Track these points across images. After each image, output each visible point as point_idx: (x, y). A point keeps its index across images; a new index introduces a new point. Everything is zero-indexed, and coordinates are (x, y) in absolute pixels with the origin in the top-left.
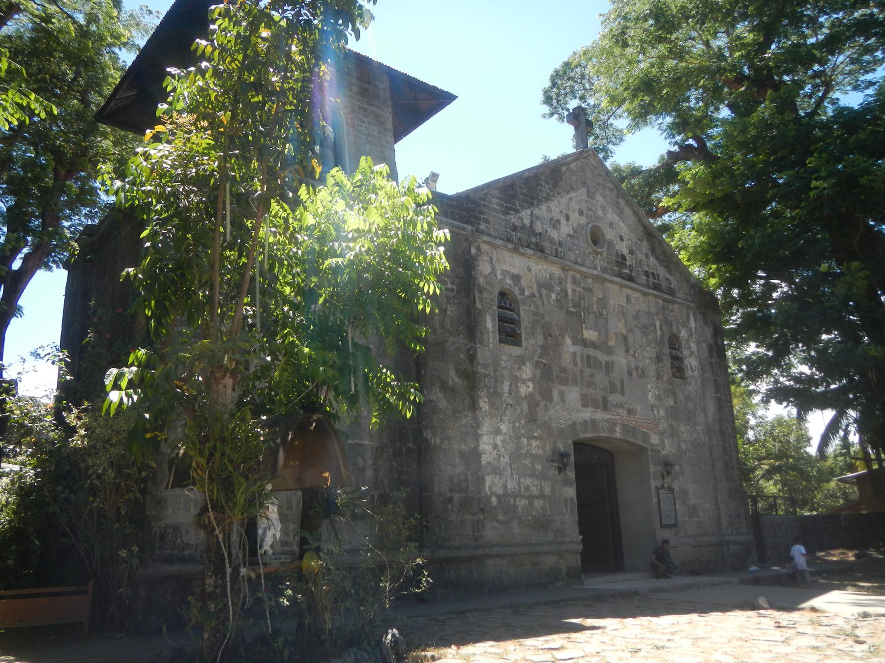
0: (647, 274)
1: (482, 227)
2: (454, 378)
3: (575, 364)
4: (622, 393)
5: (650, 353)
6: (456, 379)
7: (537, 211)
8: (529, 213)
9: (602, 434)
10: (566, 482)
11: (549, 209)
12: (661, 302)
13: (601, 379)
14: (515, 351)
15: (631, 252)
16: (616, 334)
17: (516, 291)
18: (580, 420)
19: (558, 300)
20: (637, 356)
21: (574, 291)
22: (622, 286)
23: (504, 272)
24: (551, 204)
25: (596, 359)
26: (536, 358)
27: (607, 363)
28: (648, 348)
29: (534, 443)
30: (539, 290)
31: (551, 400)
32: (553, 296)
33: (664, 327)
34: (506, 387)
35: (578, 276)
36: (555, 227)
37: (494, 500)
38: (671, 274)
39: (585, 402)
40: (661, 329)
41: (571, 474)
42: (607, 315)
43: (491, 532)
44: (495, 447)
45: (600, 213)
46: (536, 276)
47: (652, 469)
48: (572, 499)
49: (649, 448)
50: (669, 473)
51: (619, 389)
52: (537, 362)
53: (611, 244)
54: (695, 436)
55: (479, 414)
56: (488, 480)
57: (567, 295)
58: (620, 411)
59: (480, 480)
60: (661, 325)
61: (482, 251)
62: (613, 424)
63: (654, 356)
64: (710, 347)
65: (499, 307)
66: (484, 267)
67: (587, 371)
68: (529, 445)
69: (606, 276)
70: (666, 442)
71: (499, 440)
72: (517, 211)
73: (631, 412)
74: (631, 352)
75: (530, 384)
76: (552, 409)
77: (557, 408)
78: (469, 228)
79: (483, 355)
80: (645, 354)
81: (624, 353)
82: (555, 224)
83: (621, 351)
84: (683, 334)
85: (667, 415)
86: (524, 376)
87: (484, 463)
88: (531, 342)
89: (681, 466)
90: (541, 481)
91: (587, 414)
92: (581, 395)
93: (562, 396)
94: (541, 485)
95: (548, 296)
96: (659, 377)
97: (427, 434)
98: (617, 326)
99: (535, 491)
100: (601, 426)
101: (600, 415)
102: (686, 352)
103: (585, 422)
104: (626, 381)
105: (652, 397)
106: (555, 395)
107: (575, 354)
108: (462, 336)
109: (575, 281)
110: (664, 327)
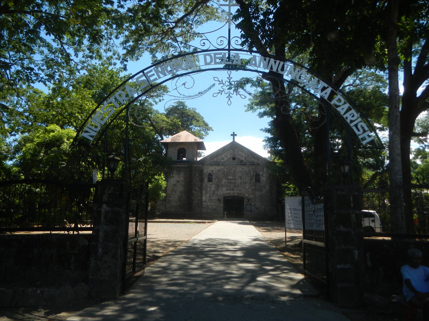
0: (250, 162)
1: (205, 164)
2: (197, 189)
4: (238, 187)
6: (198, 189)
7: (218, 158)
10: (221, 203)
11: (222, 156)
12: (254, 168)
14: (211, 183)
15: (245, 159)
17: (212, 173)
19: (222, 173)
22: (241, 167)
23: (209, 171)
24: (222, 155)
25: (231, 182)
27: (234, 182)
30: (218, 172)
31: (219, 190)
34: (209, 189)
35: (228, 167)
36: (223, 159)
37: (205, 206)
38: (258, 160)
41: (222, 202)
43: (204, 210)
44: (206, 198)
45: (236, 153)
53: (238, 159)
54: (261, 194)
55: (203, 194)
56: (204, 203)
57: (225, 171)
59: (202, 204)
64: (270, 175)
65: (208, 176)
66: (205, 170)
67: (228, 184)
70: (251, 196)
71: (206, 197)
72: (213, 159)
73: (240, 190)
78: (201, 165)
79: (204, 184)
82: (223, 159)
84: (261, 173)
88: (215, 181)
91: (228, 192)
93: (221, 189)
96: (250, 183)
97: (192, 197)
99: (213, 205)
101: (231, 192)
102: (261, 177)
103: (227, 194)
106: (220, 189)
107: (225, 182)
109: (227, 168)
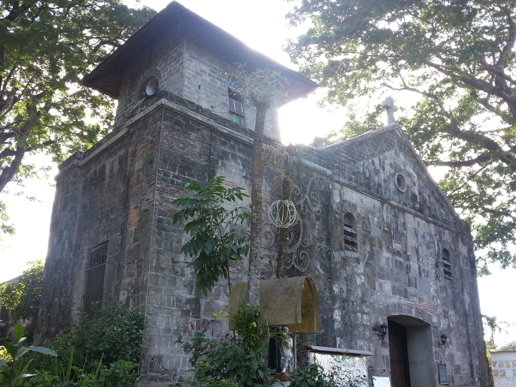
3: (389, 266)
4: (416, 287)
5: (432, 261)
8: (362, 164)
9: (404, 314)
13: (403, 277)
16: (412, 247)
18: (391, 303)
20: (424, 262)
21: (388, 217)
22: (415, 216)
26: (366, 260)
28: (430, 258)
29: (365, 317)
31: (374, 289)
32: (376, 219)
33: (440, 244)
39: (395, 291)
40: (438, 245)
41: (387, 339)
42: (406, 234)
46: (366, 206)
47: (433, 340)
48: (387, 357)
49: (432, 325)
50: (444, 343)
51: (414, 284)
52: (367, 262)
58: (415, 299)
60: (438, 243)
61: (335, 187)
62: (411, 307)
63: (434, 263)
68: (362, 318)
69: (406, 208)
70: (441, 321)
73: (421, 300)
74: (421, 259)
75: (362, 277)
76: (375, 295)
77: (378, 294)
80: (429, 261)
81: (416, 260)
83: (414, 258)
85: (442, 303)
86: (359, 271)
87: (335, 328)
89: (450, 338)
90: (369, 343)
91: (395, 299)
92: (392, 286)
94: (369, 346)
95: (373, 220)
98: (411, 241)
100: (404, 308)
101: (403, 301)
104: (418, 278)
105: (433, 291)
106: (377, 284)
108: (324, 242)
110: (440, 244)
